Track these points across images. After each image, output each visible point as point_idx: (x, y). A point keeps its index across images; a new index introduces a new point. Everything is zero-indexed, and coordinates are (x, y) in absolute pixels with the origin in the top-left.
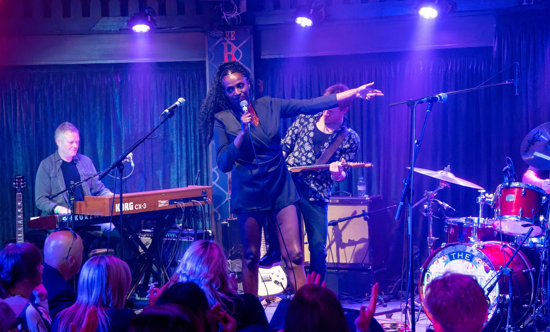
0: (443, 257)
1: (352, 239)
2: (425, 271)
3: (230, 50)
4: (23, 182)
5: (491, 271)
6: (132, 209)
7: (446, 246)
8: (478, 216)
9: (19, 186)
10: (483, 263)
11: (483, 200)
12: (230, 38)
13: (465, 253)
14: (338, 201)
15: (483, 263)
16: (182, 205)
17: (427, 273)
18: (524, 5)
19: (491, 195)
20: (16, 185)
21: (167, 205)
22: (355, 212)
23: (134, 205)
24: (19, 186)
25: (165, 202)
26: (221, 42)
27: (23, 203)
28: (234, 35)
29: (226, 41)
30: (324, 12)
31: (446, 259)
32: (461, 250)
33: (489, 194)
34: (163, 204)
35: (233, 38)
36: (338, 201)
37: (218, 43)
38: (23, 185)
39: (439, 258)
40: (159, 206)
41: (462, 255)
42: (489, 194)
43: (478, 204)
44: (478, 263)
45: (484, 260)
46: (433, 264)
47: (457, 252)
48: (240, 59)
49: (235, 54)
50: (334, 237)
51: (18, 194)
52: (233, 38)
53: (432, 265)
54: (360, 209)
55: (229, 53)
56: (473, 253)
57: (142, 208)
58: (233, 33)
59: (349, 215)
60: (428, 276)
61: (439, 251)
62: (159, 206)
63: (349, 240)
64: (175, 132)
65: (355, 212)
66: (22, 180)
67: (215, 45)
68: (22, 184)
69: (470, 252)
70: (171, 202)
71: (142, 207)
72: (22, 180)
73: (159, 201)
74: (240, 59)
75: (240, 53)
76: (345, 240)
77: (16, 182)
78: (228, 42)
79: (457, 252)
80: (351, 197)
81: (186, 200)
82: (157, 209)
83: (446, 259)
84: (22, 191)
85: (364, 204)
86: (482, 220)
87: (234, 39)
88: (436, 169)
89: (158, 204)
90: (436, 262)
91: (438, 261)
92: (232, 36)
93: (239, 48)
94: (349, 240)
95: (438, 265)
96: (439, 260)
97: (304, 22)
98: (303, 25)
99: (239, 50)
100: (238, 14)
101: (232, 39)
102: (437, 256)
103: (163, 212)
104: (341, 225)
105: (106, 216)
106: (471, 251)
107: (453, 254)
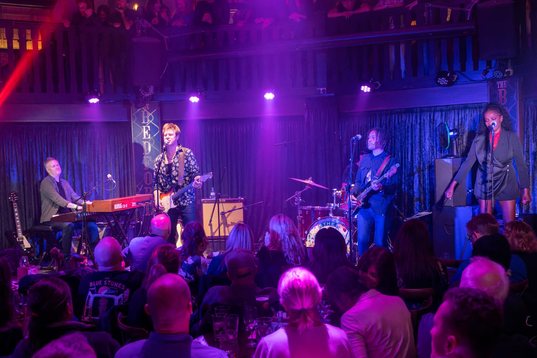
0: (318, 225)
1: (233, 222)
2: (308, 233)
3: (146, 115)
4: (16, 196)
5: (347, 231)
6: (121, 208)
7: (321, 219)
8: (333, 203)
9: (14, 199)
10: (342, 227)
11: (336, 194)
12: (146, 108)
13: (331, 222)
14: (225, 201)
15: (342, 227)
16: (143, 205)
17: (309, 234)
18: (321, 94)
19: (340, 192)
20: (11, 199)
21: (136, 205)
22: (235, 207)
23: (122, 205)
24: (14, 199)
25: (135, 203)
26: (141, 110)
27: (18, 209)
28: (149, 107)
29: (143, 110)
30: (204, 94)
31: (320, 226)
32: (329, 221)
33: (338, 191)
34: (134, 204)
35: (148, 108)
36: (225, 201)
37: (139, 111)
38: (16, 198)
39: (316, 226)
40: (133, 206)
41: (330, 223)
42: (338, 191)
43: (333, 197)
44: (340, 227)
45: (343, 225)
46: (312, 229)
47: (326, 222)
48: (152, 120)
49: (150, 116)
50: (222, 221)
51: (14, 204)
52: (148, 108)
53: (312, 230)
54: (240, 205)
55: (146, 117)
56: (336, 222)
57: (125, 207)
58: (148, 105)
59: (231, 209)
60: (309, 236)
61: (316, 222)
62: (133, 206)
63: (232, 222)
64: (111, 164)
65: (235, 207)
66: (15, 195)
67: (136, 112)
68: (15, 197)
69: (334, 221)
70: (137, 204)
71: (126, 206)
72: (15, 195)
73: (133, 203)
74: (152, 120)
75: (152, 117)
76: (229, 223)
77: (11, 197)
78: (145, 110)
79: (326, 222)
80: (230, 198)
81: (143, 202)
82: (132, 208)
83: (320, 226)
84: (16, 202)
85: (240, 202)
86: (336, 205)
87: (149, 109)
88: (304, 180)
89: (132, 204)
90: (314, 227)
91: (315, 228)
92: (147, 107)
93: (152, 114)
94: (232, 222)
95: (315, 229)
96: (316, 227)
97: (194, 99)
98: (193, 101)
99: (152, 115)
100: (150, 94)
101: (147, 109)
102: (314, 224)
103: (134, 209)
104: (226, 215)
105: (110, 212)
106: (335, 221)
107: (324, 223)
